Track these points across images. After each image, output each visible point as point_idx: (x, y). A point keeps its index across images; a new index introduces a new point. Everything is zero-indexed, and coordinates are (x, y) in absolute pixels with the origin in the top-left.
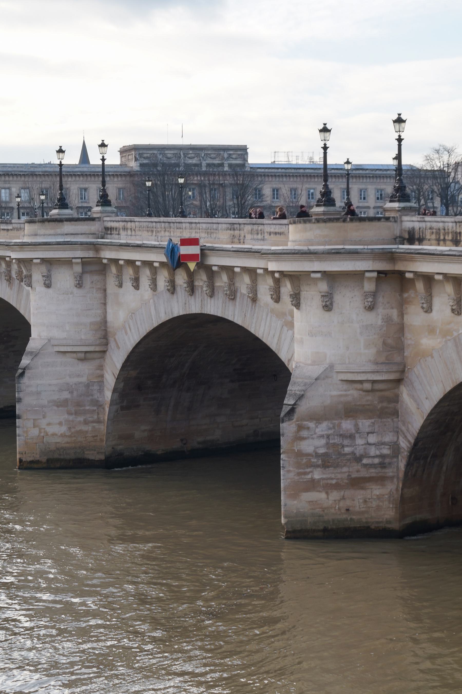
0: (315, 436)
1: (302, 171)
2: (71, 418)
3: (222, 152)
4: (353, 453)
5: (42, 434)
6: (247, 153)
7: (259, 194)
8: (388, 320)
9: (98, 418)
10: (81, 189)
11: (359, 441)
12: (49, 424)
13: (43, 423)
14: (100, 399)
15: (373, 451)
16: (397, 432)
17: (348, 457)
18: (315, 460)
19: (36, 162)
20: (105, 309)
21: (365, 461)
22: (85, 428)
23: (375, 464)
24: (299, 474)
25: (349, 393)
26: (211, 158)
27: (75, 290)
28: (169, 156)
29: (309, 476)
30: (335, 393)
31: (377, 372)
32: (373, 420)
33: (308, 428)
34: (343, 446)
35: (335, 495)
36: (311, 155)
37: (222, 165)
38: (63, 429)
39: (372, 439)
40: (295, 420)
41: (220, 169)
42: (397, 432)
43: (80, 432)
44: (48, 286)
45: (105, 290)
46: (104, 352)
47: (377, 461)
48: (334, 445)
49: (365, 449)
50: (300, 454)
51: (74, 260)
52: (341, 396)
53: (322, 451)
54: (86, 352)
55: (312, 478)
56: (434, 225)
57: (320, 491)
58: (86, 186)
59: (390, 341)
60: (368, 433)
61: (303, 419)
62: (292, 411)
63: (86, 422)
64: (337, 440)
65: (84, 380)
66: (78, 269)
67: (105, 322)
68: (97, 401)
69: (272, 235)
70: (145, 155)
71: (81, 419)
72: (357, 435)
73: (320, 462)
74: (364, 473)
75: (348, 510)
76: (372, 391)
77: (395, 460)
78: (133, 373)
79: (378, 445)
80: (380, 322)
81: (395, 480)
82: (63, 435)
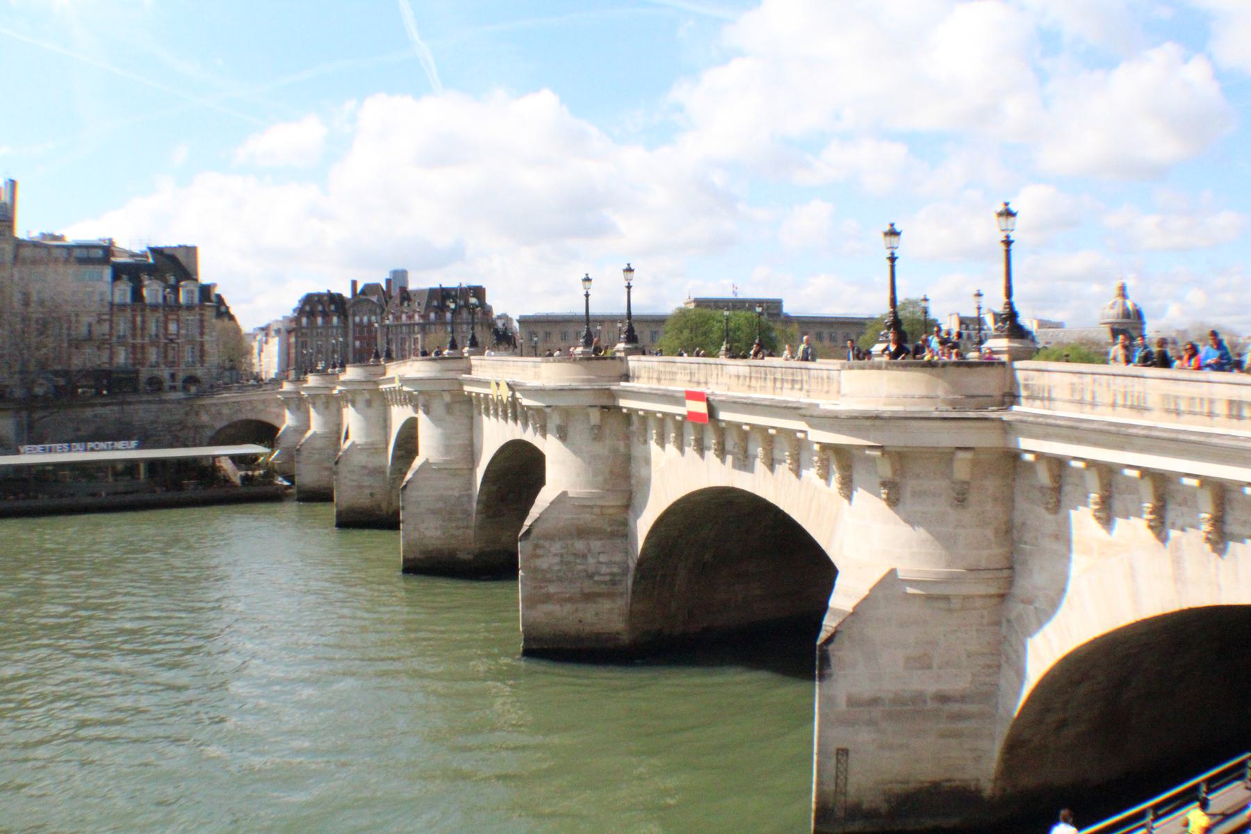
8: (615, 451)
11: (591, 560)
12: (427, 529)
14: (469, 509)
15: (604, 569)
16: (626, 552)
21: (596, 578)
22: (457, 533)
24: (535, 588)
25: (582, 516)
30: (569, 516)
32: (603, 542)
34: (576, 564)
35: (568, 607)
38: (439, 533)
39: (603, 558)
43: (453, 536)
47: (608, 578)
52: (573, 519)
54: (456, 469)
60: (599, 553)
61: (539, 539)
63: (458, 528)
64: (571, 558)
68: (467, 511)
71: (454, 525)
72: (589, 555)
74: (596, 589)
78: (494, 488)
79: (609, 564)
81: (625, 596)
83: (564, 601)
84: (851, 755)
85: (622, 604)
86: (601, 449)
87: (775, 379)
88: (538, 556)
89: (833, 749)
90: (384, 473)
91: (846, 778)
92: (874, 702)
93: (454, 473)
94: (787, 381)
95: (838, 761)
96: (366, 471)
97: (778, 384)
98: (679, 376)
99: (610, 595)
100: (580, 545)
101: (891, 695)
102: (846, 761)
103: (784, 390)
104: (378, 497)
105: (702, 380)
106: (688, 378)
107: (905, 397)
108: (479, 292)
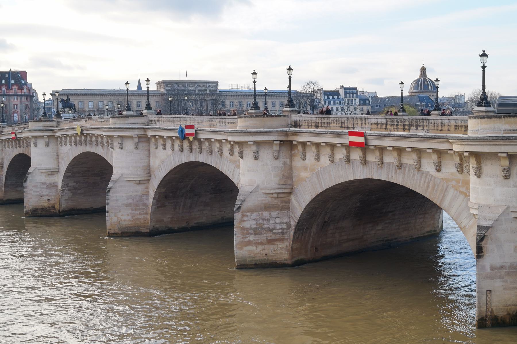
0: (250, 220)
1: (244, 93)
2: (133, 212)
3: (206, 84)
4: (269, 228)
5: (119, 220)
7: (224, 104)
8: (285, 164)
9: (146, 212)
10: (138, 102)
11: (272, 222)
12: (122, 215)
13: (119, 215)
14: (147, 203)
15: (278, 227)
16: (289, 217)
17: (266, 229)
18: (251, 231)
19: (116, 89)
20: (149, 159)
21: (274, 231)
22: (140, 217)
23: (279, 233)
24: (243, 238)
25: (266, 199)
26: (200, 87)
27: (135, 150)
28: (180, 86)
29: (248, 239)
30: (260, 199)
31: (280, 189)
32: (278, 212)
33: (247, 216)
34: (264, 224)
35: (260, 248)
36: (248, 86)
37: (206, 90)
38: (129, 217)
39: (278, 221)
40: (241, 212)
41: (205, 92)
42: (289, 217)
43: (138, 219)
44: (121, 148)
45: (149, 150)
46: (149, 180)
47: (280, 231)
48: (260, 224)
49: (274, 225)
50: (243, 228)
51: (134, 136)
52: (263, 200)
53: (254, 227)
55: (249, 240)
56: (307, 119)
57: (253, 246)
58: (140, 100)
59: (286, 174)
60: (276, 218)
61: (245, 212)
62: (239, 207)
63: (140, 214)
64: (261, 221)
65: (139, 193)
66: (136, 140)
67: (149, 166)
68: (146, 204)
69: (229, 124)
70: (169, 86)
71: (138, 212)
72: (270, 219)
73: (253, 232)
74: (274, 237)
75: (266, 255)
76: (278, 198)
77: (289, 230)
78: (163, 190)
80: (281, 165)
81: (289, 240)
82: (129, 221)
83: (257, 244)
84: (493, 293)
85: (287, 244)
86: (279, 163)
87: (404, 125)
88: (244, 221)
89: (485, 290)
91: (491, 304)
93: (140, 182)
94: (413, 126)
95: (487, 296)
96: (45, 186)
97: (407, 127)
98: (332, 125)
99: (282, 240)
100: (266, 214)
101: (509, 264)
102: (491, 296)
103: (411, 130)
104: (52, 202)
105: (350, 126)
106: (340, 125)
107: (513, 130)
108: (23, 75)
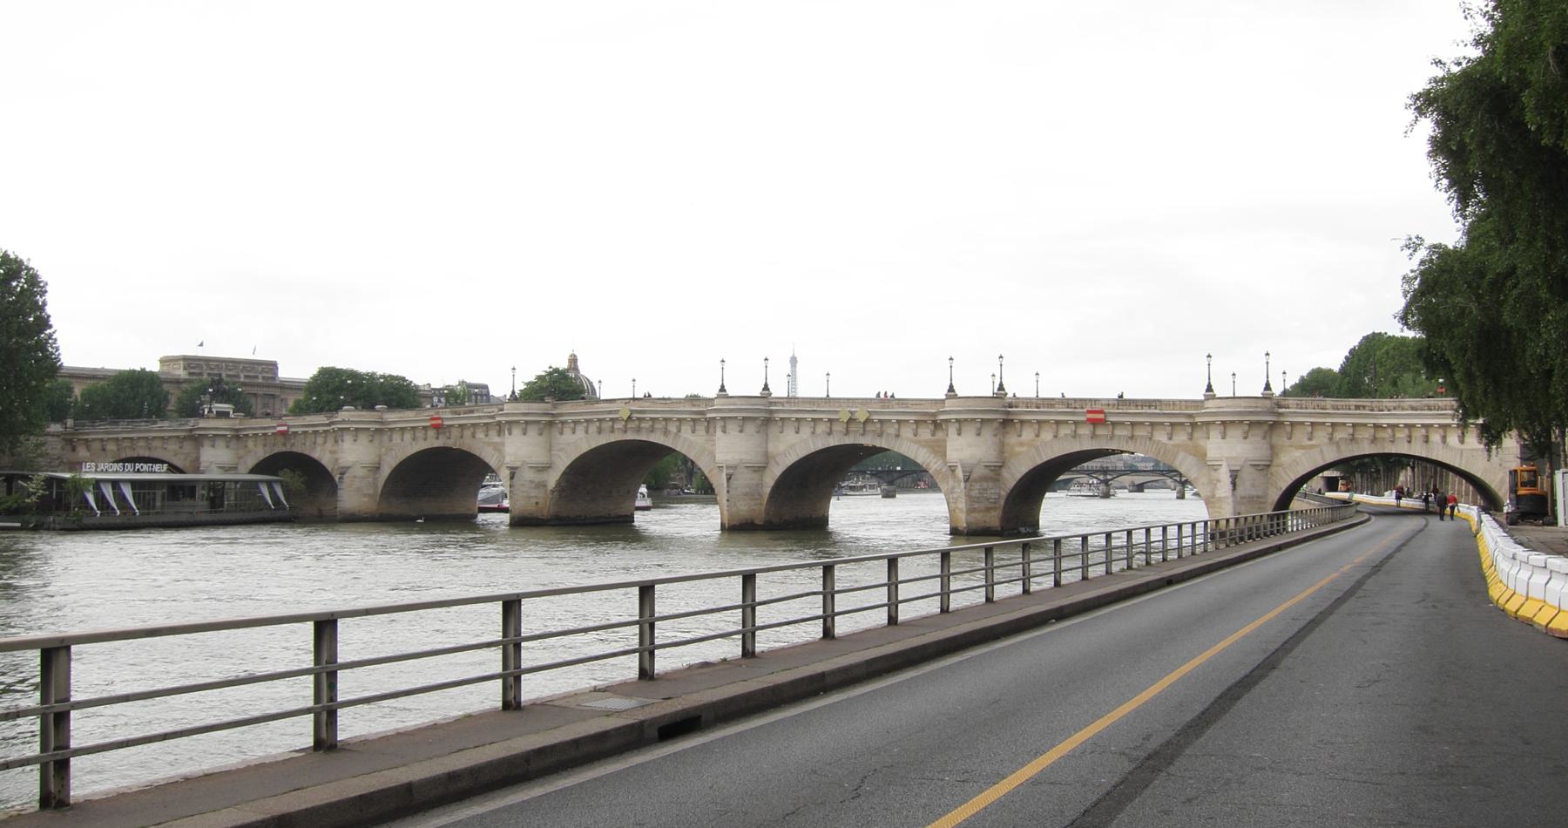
6: (277, 368)
11: (989, 492)
15: (993, 497)
22: (755, 507)
27: (755, 434)
35: (981, 514)
37: (201, 374)
39: (993, 491)
43: (754, 509)
46: (765, 467)
63: (756, 505)
64: (982, 491)
65: (755, 482)
79: (995, 493)
90: (545, 486)
92: (1244, 498)
99: (994, 509)
100: (985, 485)
